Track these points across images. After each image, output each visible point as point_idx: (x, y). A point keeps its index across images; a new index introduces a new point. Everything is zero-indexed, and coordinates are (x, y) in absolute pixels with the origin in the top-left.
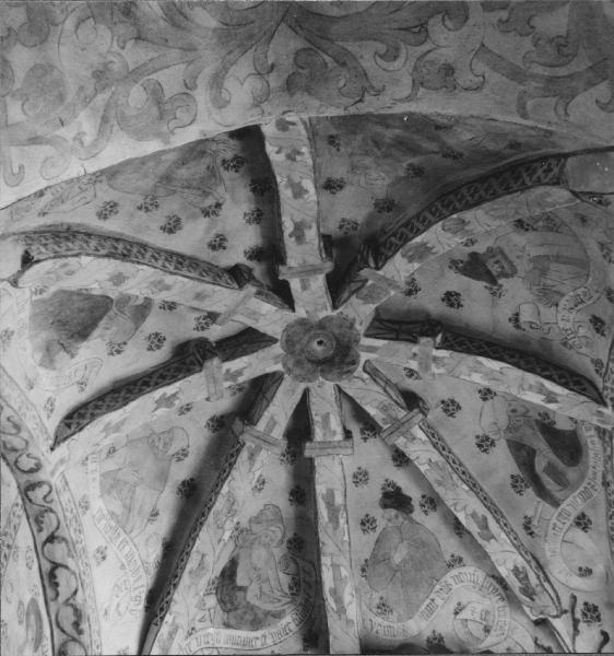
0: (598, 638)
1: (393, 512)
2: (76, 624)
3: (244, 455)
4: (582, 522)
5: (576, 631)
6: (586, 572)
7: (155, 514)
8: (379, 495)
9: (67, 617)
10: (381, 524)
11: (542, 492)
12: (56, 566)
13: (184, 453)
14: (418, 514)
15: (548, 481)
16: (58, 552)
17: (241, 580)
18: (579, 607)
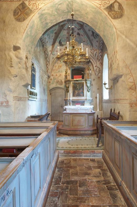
0: (96, 52)
1: (78, 35)
2: (46, 50)
3: (62, 31)
4: (97, 41)
5: (94, 51)
6: (96, 46)
7: (52, 36)
8: (77, 33)
9: (45, 49)
10: (77, 36)
11: (94, 37)
12: (44, 45)
13: (55, 30)
14: (81, 36)
15: (95, 36)
16: (44, 44)
17: (61, 42)
18: (95, 49)
